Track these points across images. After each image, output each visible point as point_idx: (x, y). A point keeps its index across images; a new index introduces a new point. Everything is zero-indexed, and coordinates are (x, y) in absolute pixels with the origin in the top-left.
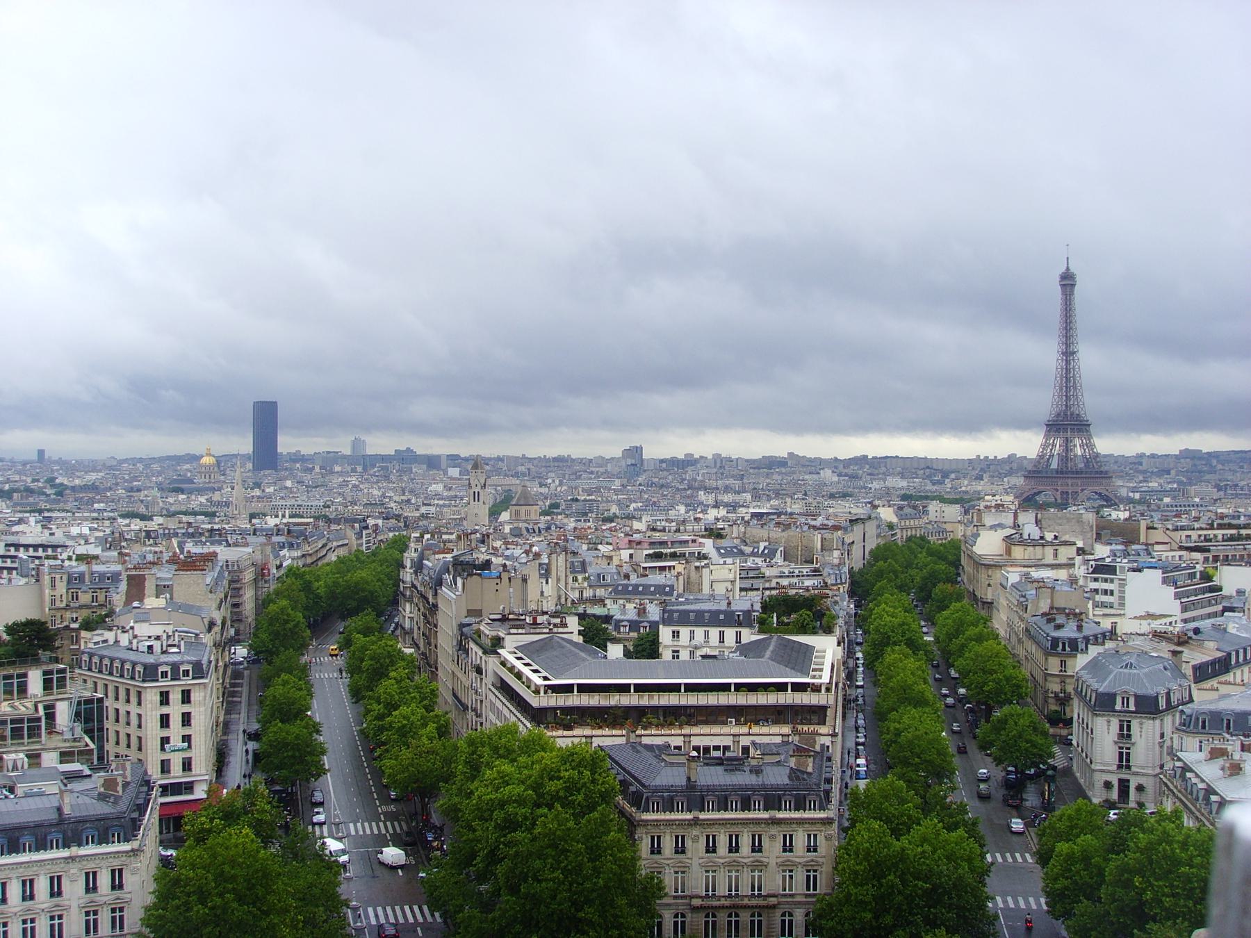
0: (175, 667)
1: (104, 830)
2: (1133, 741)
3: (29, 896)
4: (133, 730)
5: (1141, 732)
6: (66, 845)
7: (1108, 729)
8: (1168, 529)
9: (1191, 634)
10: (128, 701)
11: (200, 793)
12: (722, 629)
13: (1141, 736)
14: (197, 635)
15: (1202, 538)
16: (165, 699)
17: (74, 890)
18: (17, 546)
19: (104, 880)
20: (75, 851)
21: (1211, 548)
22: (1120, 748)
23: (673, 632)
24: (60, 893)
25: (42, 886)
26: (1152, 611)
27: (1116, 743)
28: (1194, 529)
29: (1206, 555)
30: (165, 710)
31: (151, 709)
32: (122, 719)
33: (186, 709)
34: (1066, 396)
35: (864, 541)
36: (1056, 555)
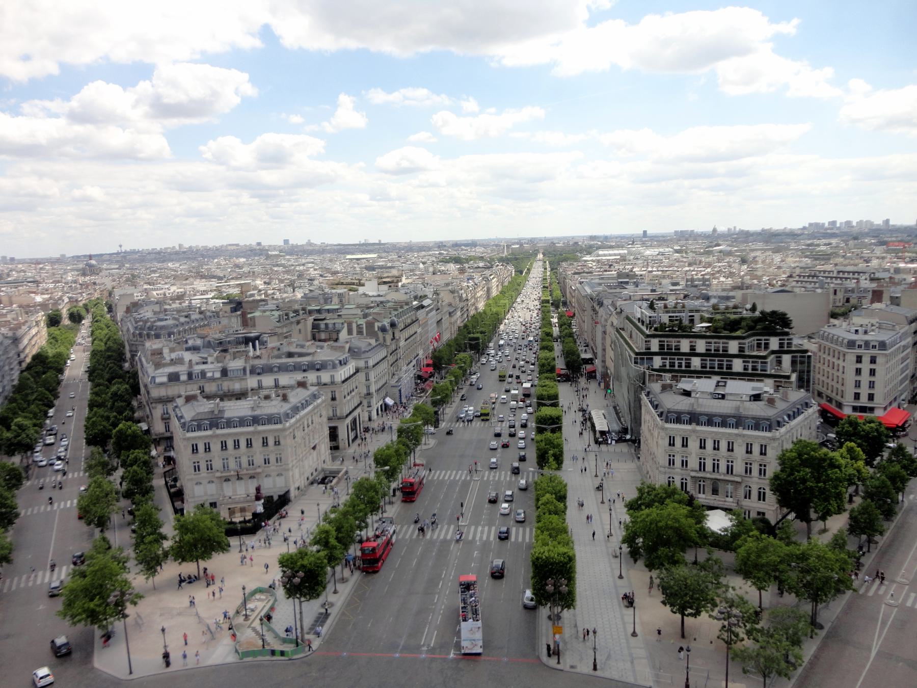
0: (867, 343)
1: (757, 424)
3: (716, 448)
4: (840, 374)
6: (737, 428)
10: (839, 358)
11: (879, 413)
14: (894, 326)
16: (859, 359)
17: (739, 450)
18: (844, 272)
19: (756, 449)
20: (740, 431)
24: (732, 450)
25: (723, 445)
30: (859, 366)
31: (850, 365)
32: (836, 368)
33: (873, 366)
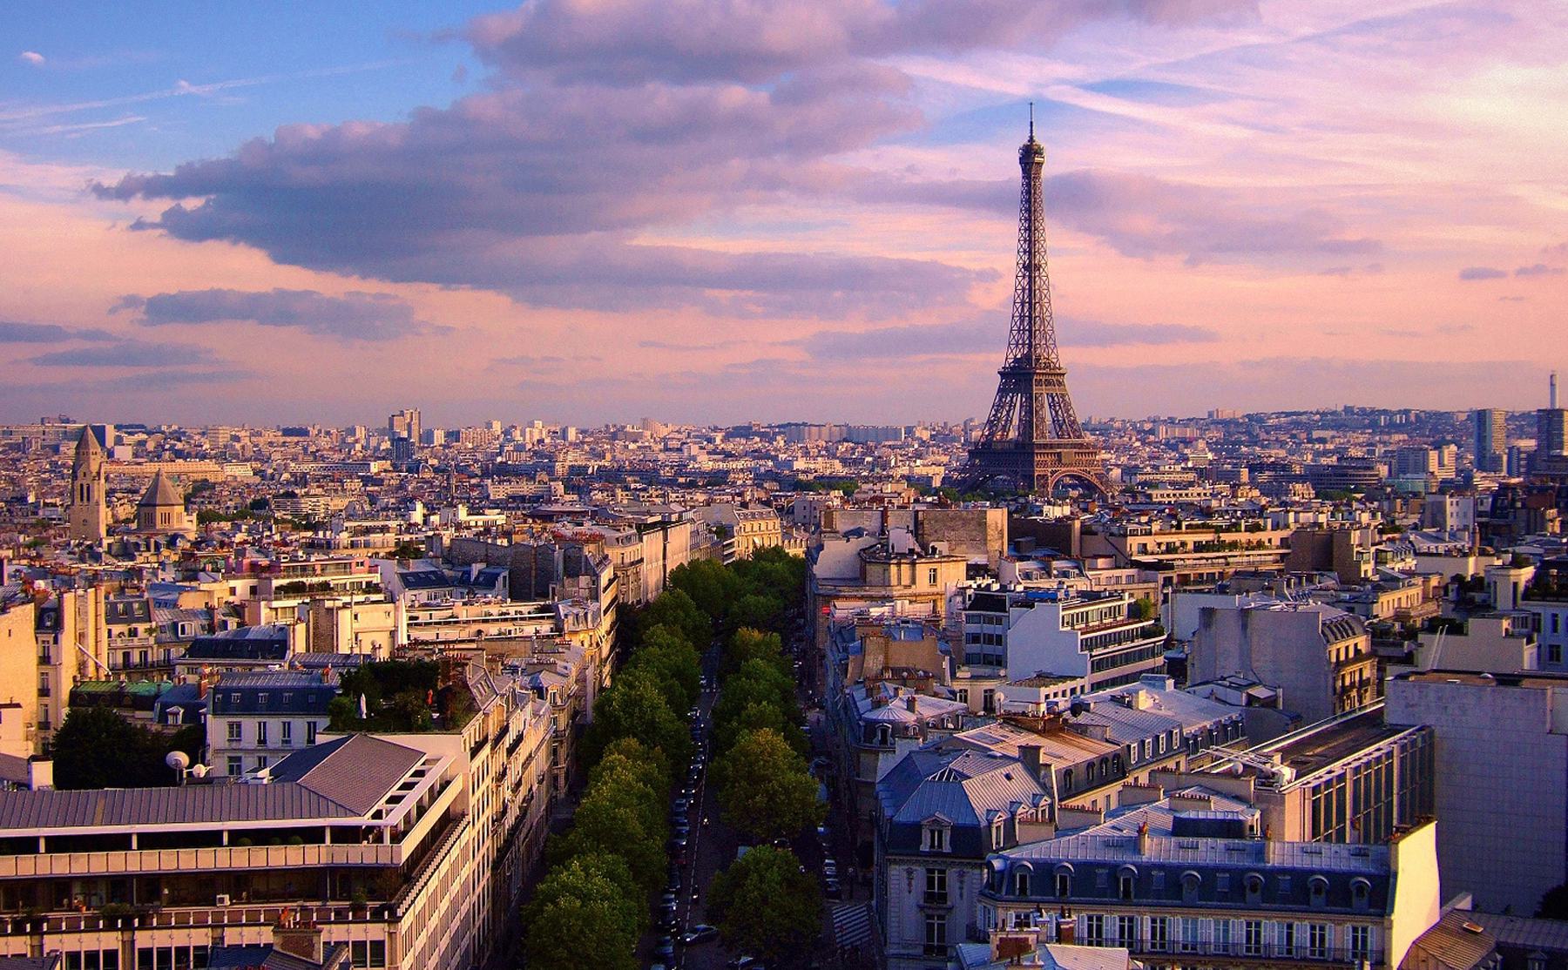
2: (949, 903)
5: (961, 888)
7: (910, 884)
8: (1112, 534)
9: (1067, 715)
12: (313, 720)
13: (961, 895)
15: (1163, 547)
21: (1176, 563)
22: (930, 917)
23: (231, 725)
26: (1047, 668)
27: (921, 908)
28: (1149, 533)
29: (1169, 574)
34: (1030, 331)
35: (664, 558)
36: (933, 579)
